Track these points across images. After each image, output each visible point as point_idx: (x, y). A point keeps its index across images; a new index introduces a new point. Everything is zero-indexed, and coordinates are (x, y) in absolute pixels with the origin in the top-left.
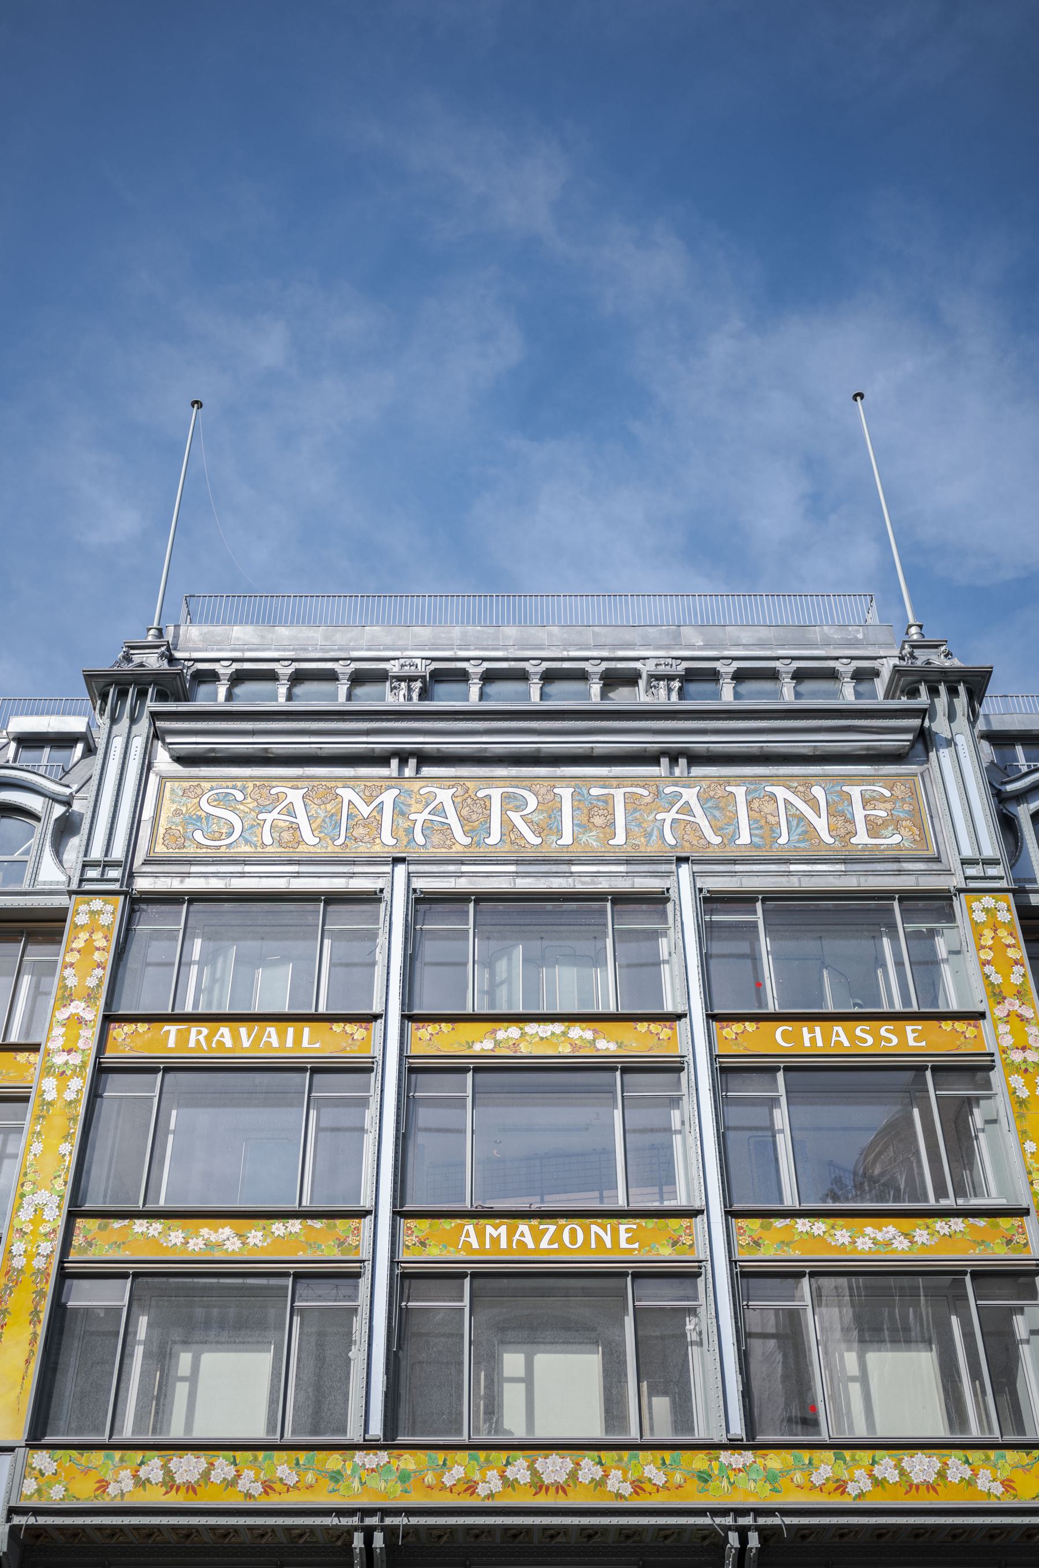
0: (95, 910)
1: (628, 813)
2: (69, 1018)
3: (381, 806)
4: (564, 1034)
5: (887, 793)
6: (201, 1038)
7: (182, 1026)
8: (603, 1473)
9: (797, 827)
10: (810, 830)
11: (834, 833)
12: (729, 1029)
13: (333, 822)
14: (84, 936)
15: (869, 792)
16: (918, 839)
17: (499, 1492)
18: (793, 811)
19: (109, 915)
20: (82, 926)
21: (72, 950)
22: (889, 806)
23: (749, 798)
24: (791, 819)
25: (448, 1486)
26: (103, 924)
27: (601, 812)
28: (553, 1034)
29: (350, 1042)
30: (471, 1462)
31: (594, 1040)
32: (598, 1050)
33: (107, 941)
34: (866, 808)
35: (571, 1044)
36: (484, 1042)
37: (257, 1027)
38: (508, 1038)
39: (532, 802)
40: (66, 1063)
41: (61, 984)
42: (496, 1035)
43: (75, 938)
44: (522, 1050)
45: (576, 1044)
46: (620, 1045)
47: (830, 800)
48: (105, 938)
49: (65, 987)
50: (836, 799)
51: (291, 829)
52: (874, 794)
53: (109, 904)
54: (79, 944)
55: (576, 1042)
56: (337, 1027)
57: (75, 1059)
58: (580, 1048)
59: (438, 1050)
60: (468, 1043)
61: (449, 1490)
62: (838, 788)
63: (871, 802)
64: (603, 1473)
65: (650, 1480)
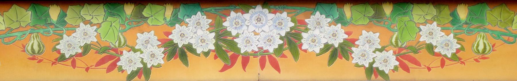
8: (346, 36)
17: (159, 66)
25: (67, 56)
30: (110, 19)
61: (69, 62)
64: (346, 36)
65: (430, 48)
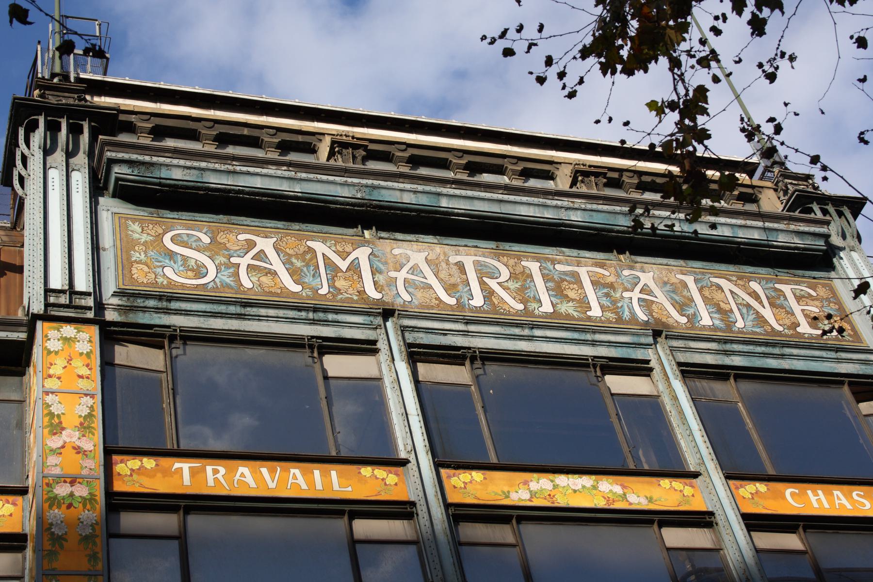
0: (68, 337)
1: (596, 289)
2: (63, 447)
3: (357, 261)
4: (595, 487)
5: (813, 293)
6: (219, 476)
7: (196, 464)
9: (748, 315)
10: (760, 320)
11: (781, 322)
12: (743, 489)
13: (312, 273)
14: (60, 362)
15: (798, 291)
16: (852, 333)
18: (740, 301)
19: (86, 343)
20: (57, 353)
21: (50, 376)
22: (817, 303)
23: (699, 285)
24: (740, 307)
26: (81, 351)
27: (571, 286)
28: (584, 487)
29: (383, 487)
31: (625, 494)
32: (631, 504)
33: (90, 369)
34: (800, 303)
35: (604, 498)
36: (520, 492)
37: (278, 466)
38: (542, 490)
39: (505, 274)
40: (72, 495)
41: (46, 412)
42: (529, 486)
43: (51, 364)
44: (559, 501)
45: (609, 498)
46: (650, 500)
47: (769, 295)
48: (87, 366)
49: (51, 415)
50: (773, 294)
51: (269, 275)
52: (802, 293)
53: (83, 332)
54: (56, 370)
55: (609, 496)
56: (367, 471)
57: (81, 491)
58: (614, 502)
59: (476, 498)
60: (504, 492)
62: (771, 285)
63: (803, 299)
